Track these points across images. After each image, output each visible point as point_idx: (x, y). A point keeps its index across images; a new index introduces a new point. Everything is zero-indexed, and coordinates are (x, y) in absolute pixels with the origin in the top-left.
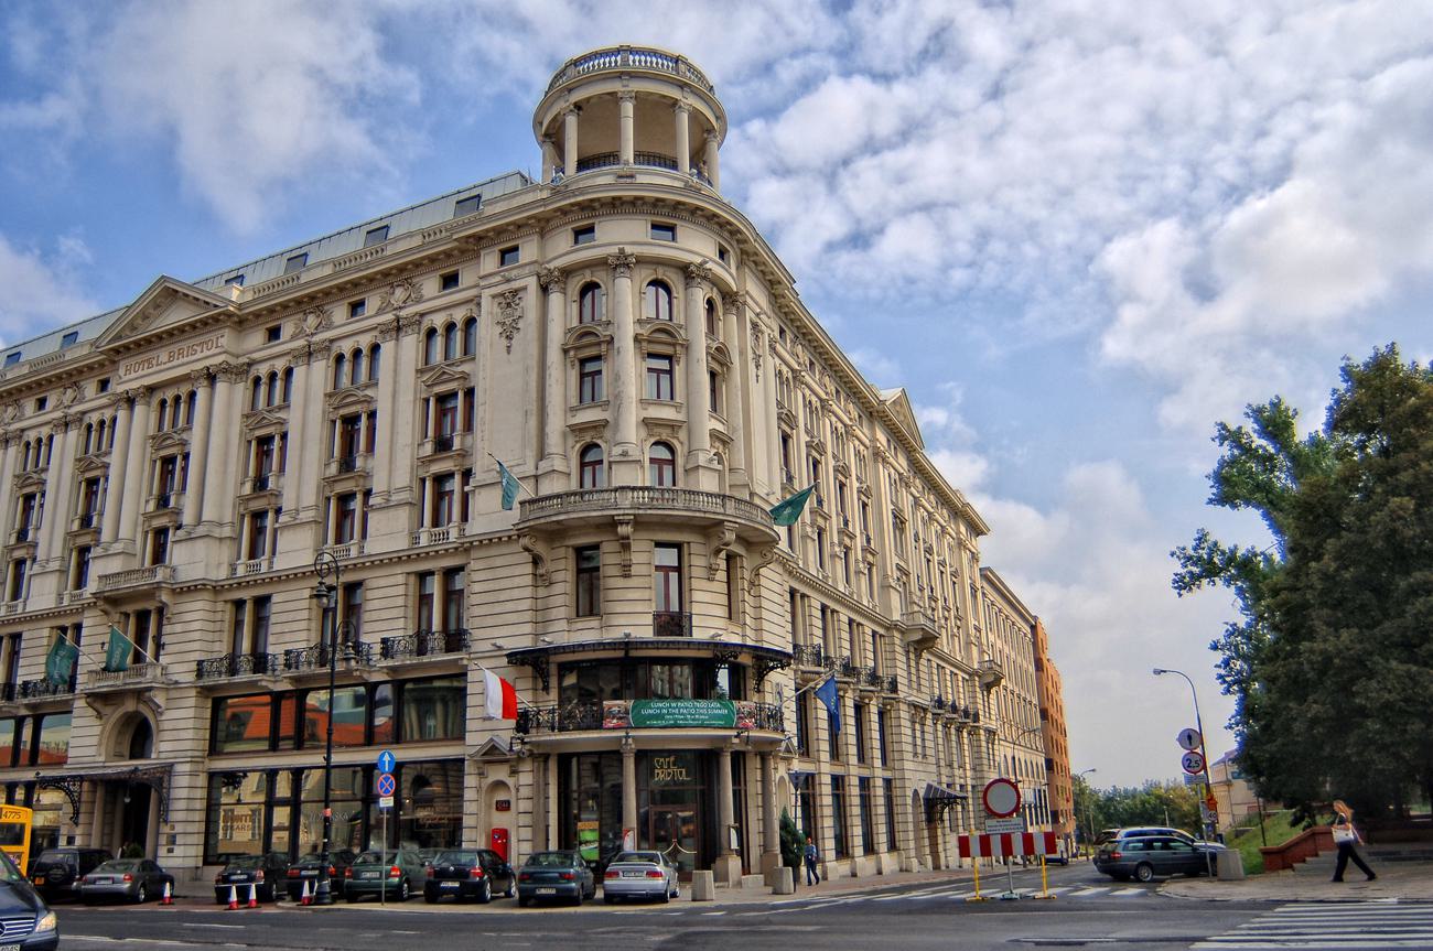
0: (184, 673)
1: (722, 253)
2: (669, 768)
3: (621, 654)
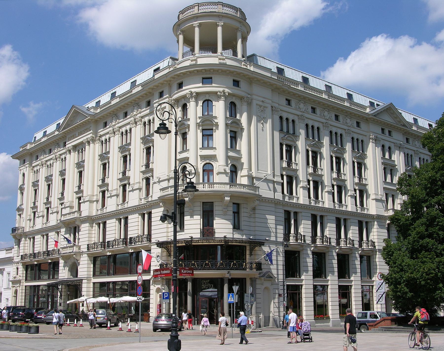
0: (84, 248)
1: (236, 83)
2: (207, 284)
3: (184, 244)
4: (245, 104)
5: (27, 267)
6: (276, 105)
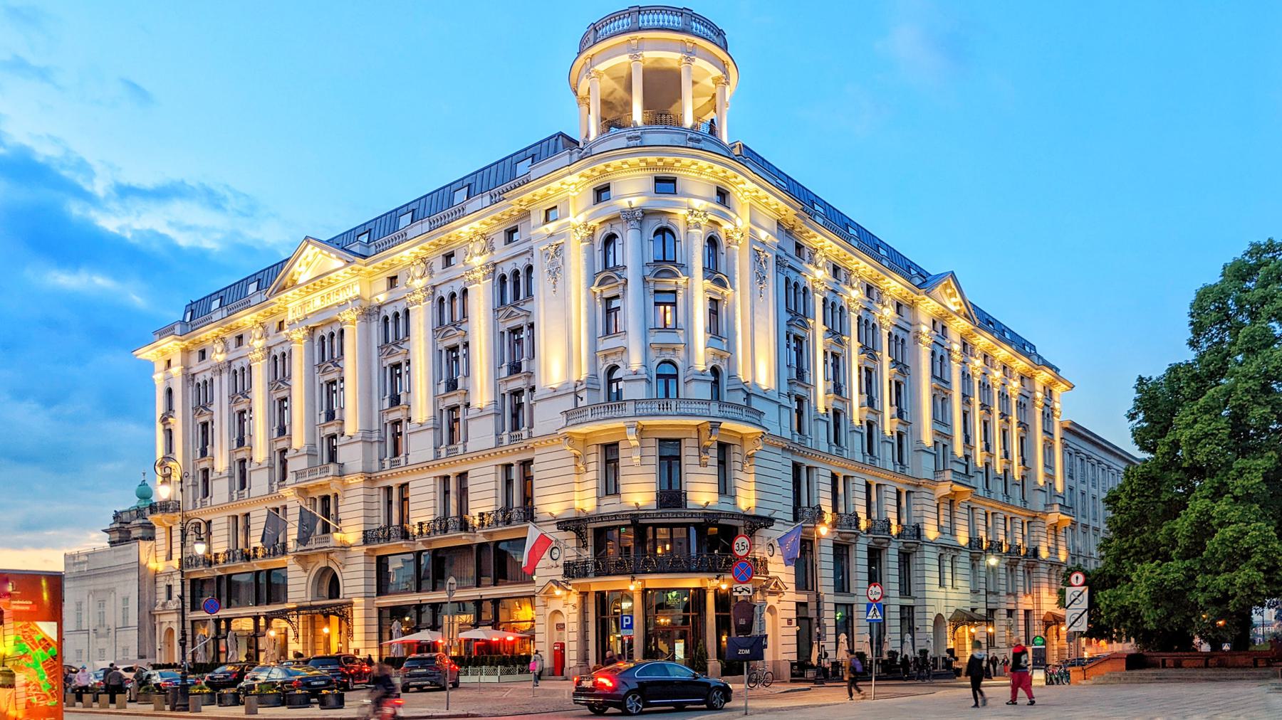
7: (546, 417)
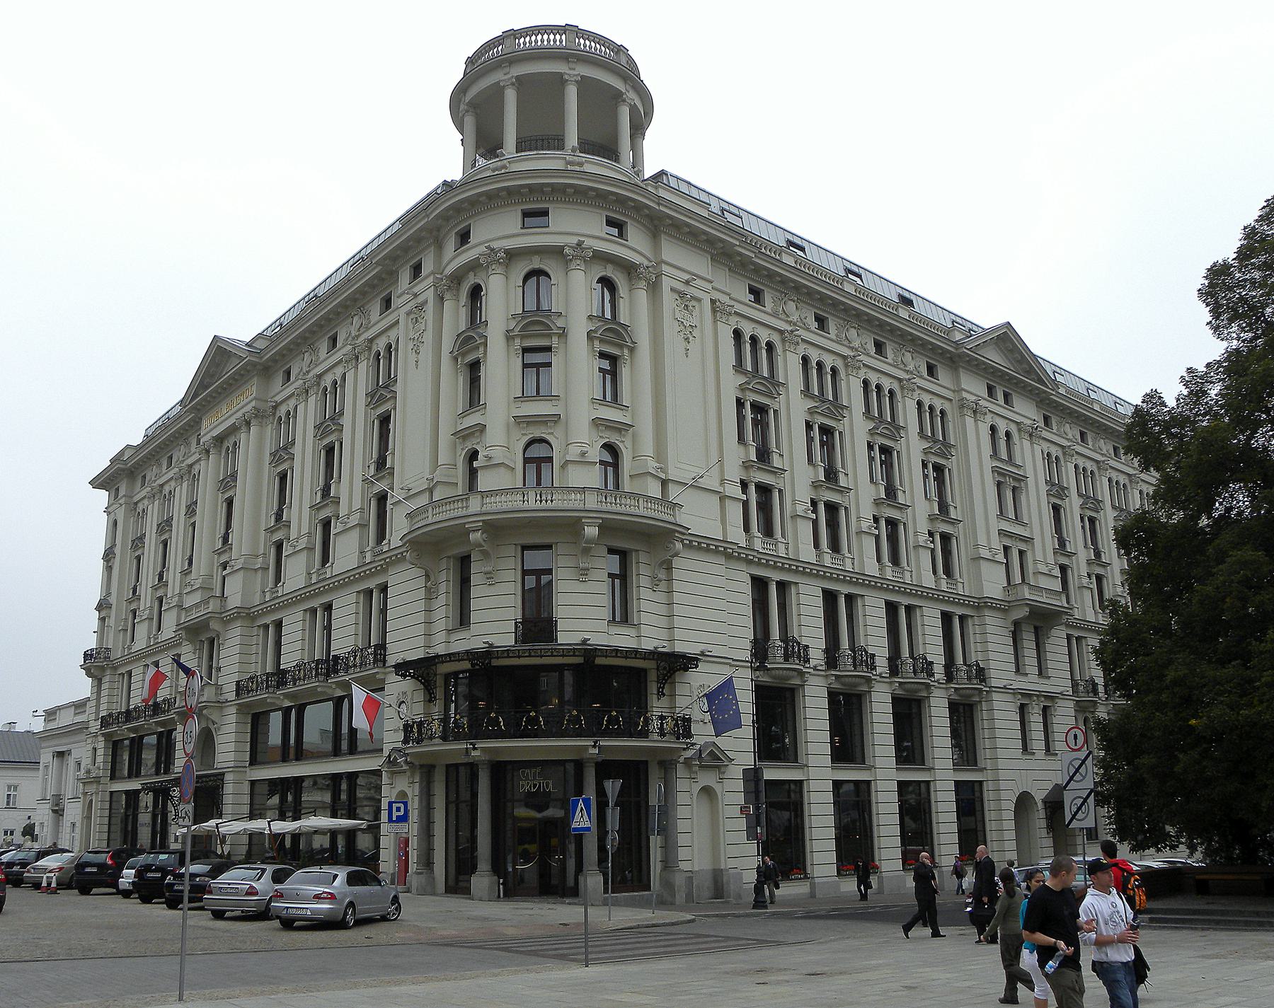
0: (230, 693)
4: (643, 284)
5: (115, 746)
6: (725, 299)
7: (399, 527)
